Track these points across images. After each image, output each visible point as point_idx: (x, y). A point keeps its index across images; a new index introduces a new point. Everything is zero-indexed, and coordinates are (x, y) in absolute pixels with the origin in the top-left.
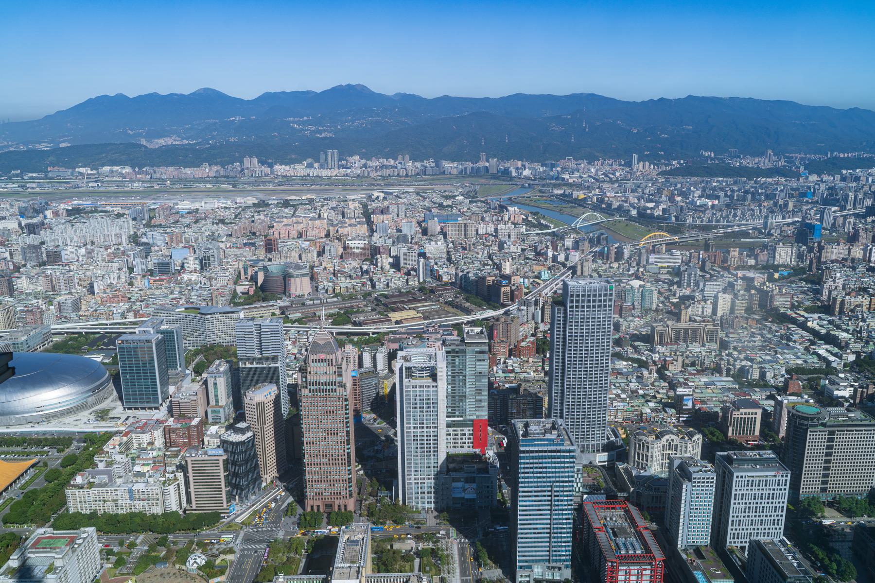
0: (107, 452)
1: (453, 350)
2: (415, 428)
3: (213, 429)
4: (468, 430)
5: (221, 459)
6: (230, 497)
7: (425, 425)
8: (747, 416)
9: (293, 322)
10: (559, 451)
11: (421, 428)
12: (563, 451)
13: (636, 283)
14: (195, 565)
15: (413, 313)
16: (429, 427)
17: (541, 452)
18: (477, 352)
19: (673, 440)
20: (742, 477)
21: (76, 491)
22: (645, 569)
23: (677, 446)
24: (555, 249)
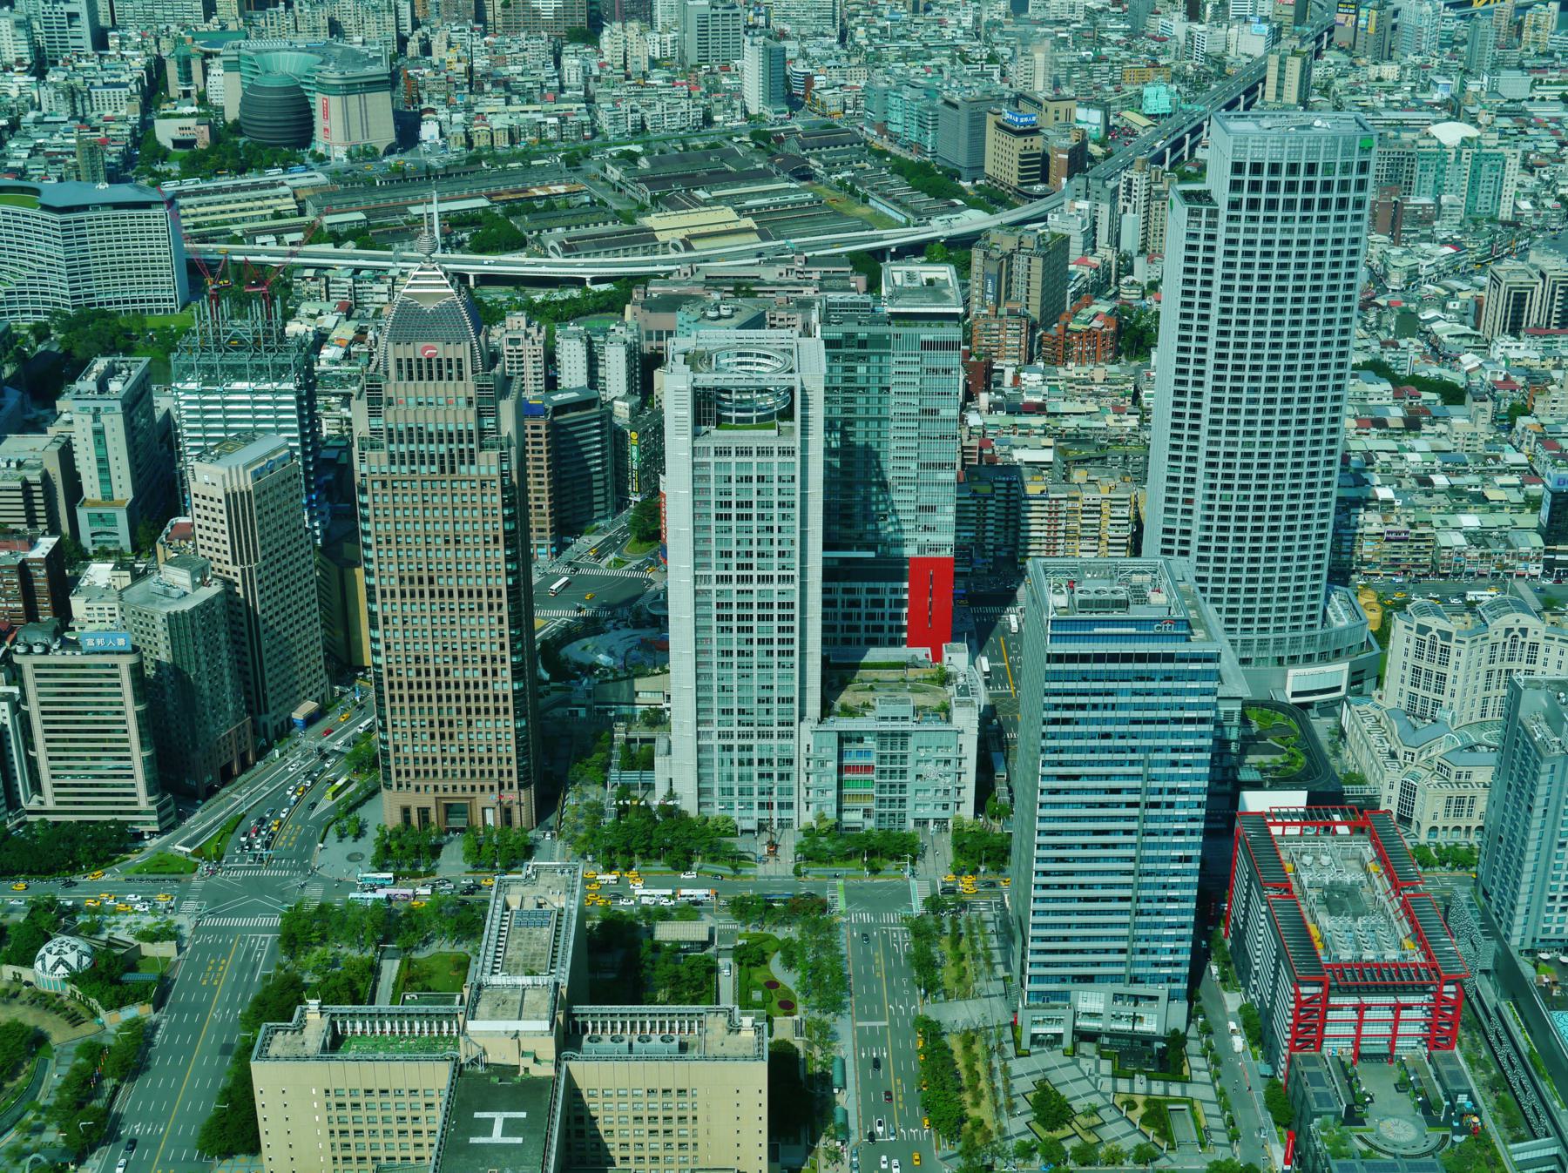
1: (850, 336)
2: (720, 579)
7: (755, 573)
9: (337, 239)
10: (1169, 658)
11: (741, 579)
13: (1450, 133)
14: (61, 969)
15: (725, 216)
16: (769, 579)
18: (926, 345)
19: (1524, 631)
23: (1534, 647)
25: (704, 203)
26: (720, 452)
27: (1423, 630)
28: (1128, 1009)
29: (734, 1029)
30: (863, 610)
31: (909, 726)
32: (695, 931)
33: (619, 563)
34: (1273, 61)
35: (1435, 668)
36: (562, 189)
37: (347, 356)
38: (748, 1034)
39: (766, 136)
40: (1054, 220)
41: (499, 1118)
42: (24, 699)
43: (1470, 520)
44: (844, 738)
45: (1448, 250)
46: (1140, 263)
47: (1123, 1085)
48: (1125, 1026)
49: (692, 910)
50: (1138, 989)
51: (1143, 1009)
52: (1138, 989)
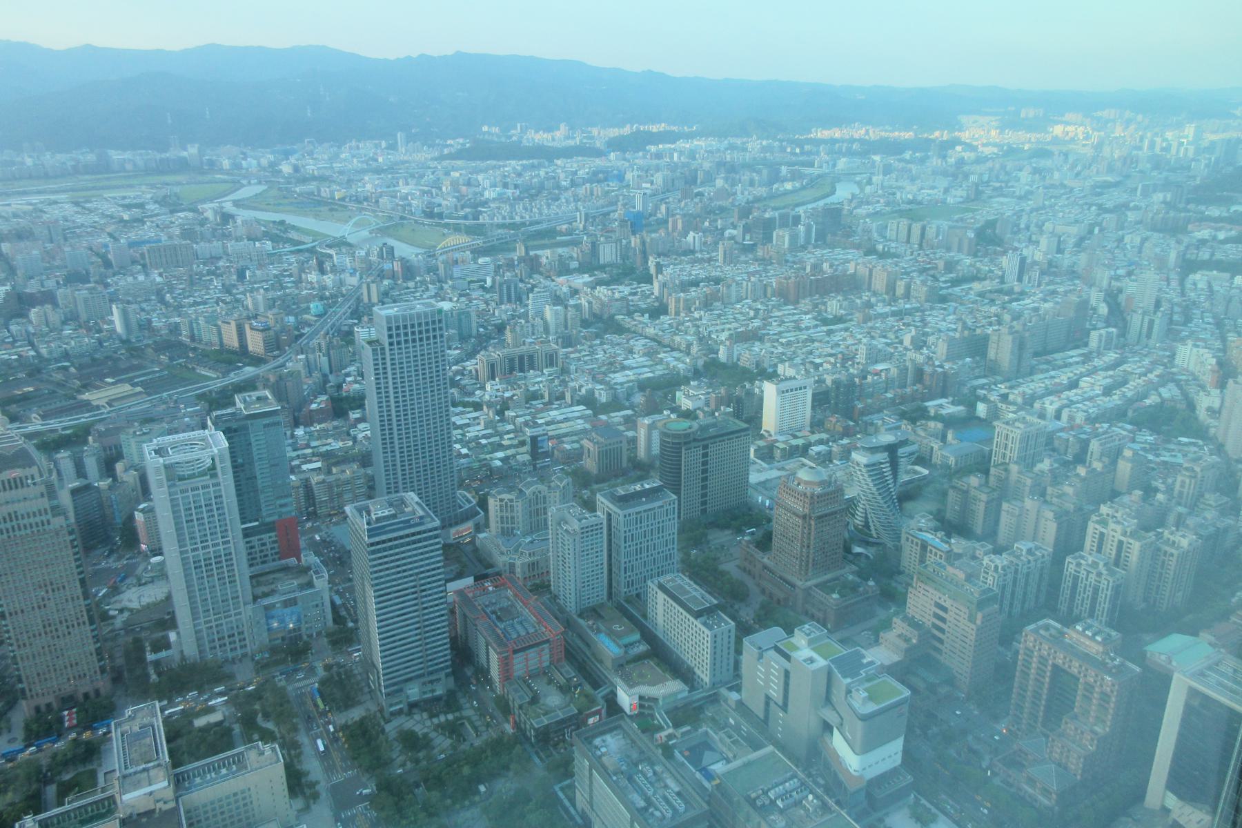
2: (193, 550)
4: (269, 537)
7: (210, 543)
10: (419, 533)
12: (424, 532)
15: (126, 388)
16: (218, 544)
17: (396, 539)
18: (265, 426)
23: (545, 497)
24: (322, 271)
25: (113, 384)
26: (182, 492)
27: (501, 500)
28: (429, 687)
29: (262, 753)
30: (257, 549)
31: (297, 594)
33: (119, 558)
34: (365, 286)
36: (31, 389)
38: (268, 753)
39: (136, 349)
40: (289, 364)
43: (500, 454)
44: (267, 608)
46: (331, 377)
47: (435, 721)
48: (429, 695)
49: (211, 710)
50: (431, 678)
52: (431, 678)
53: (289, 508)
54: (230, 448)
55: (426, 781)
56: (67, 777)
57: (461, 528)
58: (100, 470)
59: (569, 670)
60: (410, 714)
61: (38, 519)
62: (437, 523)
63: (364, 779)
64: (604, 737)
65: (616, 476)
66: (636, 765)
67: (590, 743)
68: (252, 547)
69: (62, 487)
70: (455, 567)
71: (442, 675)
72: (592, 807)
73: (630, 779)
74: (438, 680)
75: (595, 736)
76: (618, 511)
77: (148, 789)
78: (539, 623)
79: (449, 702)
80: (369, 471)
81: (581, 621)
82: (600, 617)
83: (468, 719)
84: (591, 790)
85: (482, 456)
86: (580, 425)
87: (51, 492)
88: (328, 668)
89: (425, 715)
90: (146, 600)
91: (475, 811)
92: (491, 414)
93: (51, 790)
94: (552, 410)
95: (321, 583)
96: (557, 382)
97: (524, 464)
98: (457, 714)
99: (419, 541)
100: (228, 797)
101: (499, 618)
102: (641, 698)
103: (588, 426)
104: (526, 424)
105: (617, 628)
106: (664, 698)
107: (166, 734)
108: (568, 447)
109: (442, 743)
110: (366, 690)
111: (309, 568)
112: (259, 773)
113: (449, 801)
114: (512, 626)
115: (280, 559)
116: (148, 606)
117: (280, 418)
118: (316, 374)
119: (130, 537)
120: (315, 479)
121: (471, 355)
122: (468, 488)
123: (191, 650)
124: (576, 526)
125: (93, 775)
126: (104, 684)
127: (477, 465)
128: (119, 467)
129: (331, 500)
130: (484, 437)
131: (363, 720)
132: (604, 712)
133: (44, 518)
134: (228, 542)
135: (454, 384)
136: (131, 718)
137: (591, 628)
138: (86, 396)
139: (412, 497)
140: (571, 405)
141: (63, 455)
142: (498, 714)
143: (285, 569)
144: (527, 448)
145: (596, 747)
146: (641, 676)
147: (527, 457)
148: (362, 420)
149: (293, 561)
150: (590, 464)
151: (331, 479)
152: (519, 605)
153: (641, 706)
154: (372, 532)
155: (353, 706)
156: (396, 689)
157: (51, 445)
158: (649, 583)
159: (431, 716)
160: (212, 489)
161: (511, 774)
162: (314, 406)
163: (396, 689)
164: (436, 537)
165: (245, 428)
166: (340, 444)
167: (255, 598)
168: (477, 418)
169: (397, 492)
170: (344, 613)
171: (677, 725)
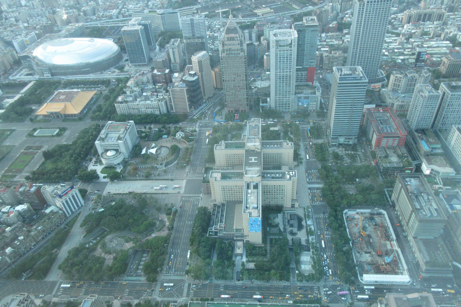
0: (129, 87)
2: (279, 72)
3: (176, 75)
4: (304, 73)
5: (185, 89)
6: (190, 107)
7: (285, 71)
8: (457, 63)
10: (359, 83)
11: (283, 72)
12: (361, 83)
15: (268, 10)
19: (415, 77)
20: (454, 95)
21: (120, 105)
22: (396, 140)
23: (416, 79)
25: (265, 7)
26: (280, 51)
27: (396, 77)
28: (347, 140)
31: (310, 95)
32: (276, 129)
33: (257, 70)
35: (398, 83)
36: (240, 6)
37: (209, 37)
38: (290, 145)
41: (253, 158)
42: (170, 95)
43: (402, 57)
44: (299, 98)
45: (396, 9)
46: (340, 14)
47: (347, 152)
48: (347, 143)
49: (274, 125)
51: (350, 140)
53: (313, 64)
54: (298, 37)
55: (338, 171)
56: (234, 133)
57: (376, 84)
58: (256, 39)
59: (404, 150)
60: (338, 147)
61: (237, 52)
62: (367, 81)
63: (318, 163)
64: (411, 179)
65: (454, 77)
66: (421, 193)
67: (404, 179)
68: (298, 75)
69: (245, 43)
70: (369, 99)
71: (353, 137)
72: (397, 201)
73: (417, 197)
74: (351, 139)
75: (407, 177)
76: (450, 92)
77: (254, 144)
78: (398, 129)
79: (354, 147)
80: (346, 55)
81: (416, 134)
82: (425, 134)
83: (359, 155)
84: (399, 195)
85: (394, 57)
86: (444, 50)
87: (241, 44)
88: (314, 123)
89: (344, 149)
90: (262, 86)
91: (353, 186)
92: (403, 39)
93: (230, 136)
94: (432, 41)
95: (318, 94)
96: (439, 29)
97: (411, 63)
98: (355, 152)
99: (358, 86)
100: (275, 154)
101: (381, 123)
102: (432, 170)
103: (448, 51)
104: (418, 46)
105: (431, 140)
106: (443, 173)
107: (262, 129)
108: (434, 59)
109: (347, 161)
110: (325, 134)
111: (315, 87)
112: (286, 150)
113: (344, 180)
114: (386, 127)
115: (306, 82)
116: (263, 88)
117: (317, 29)
118: (335, 12)
119: (261, 64)
120: (325, 54)
121: (402, 11)
122: (384, 69)
123: (273, 105)
124: (426, 94)
125: (240, 135)
126: (247, 109)
127: (390, 60)
128: (262, 38)
129: (329, 64)
130: (397, 49)
131: (322, 143)
132: (414, 170)
133: (238, 52)
134: (291, 72)
135: (390, 23)
136: (253, 122)
137: (419, 137)
138: (255, 11)
139: (360, 68)
140: (443, 41)
141: (246, 31)
142: (370, 157)
143: (307, 86)
144: (415, 57)
145: (406, 181)
146: (435, 161)
147: (414, 61)
148: (348, 34)
149: (310, 83)
150: (443, 69)
151: (331, 55)
152: (391, 120)
153: (431, 173)
154: (341, 79)
155: (320, 138)
156: (336, 138)
157: (244, 27)
158: (453, 126)
159: (346, 150)
160: (289, 52)
161: (369, 179)
162: (331, 25)
163: (336, 138)
164: (365, 86)
165: (304, 30)
166: (337, 42)
167: (296, 93)
168: (396, 40)
169: (354, 65)
170: (324, 106)
171: (444, 185)
